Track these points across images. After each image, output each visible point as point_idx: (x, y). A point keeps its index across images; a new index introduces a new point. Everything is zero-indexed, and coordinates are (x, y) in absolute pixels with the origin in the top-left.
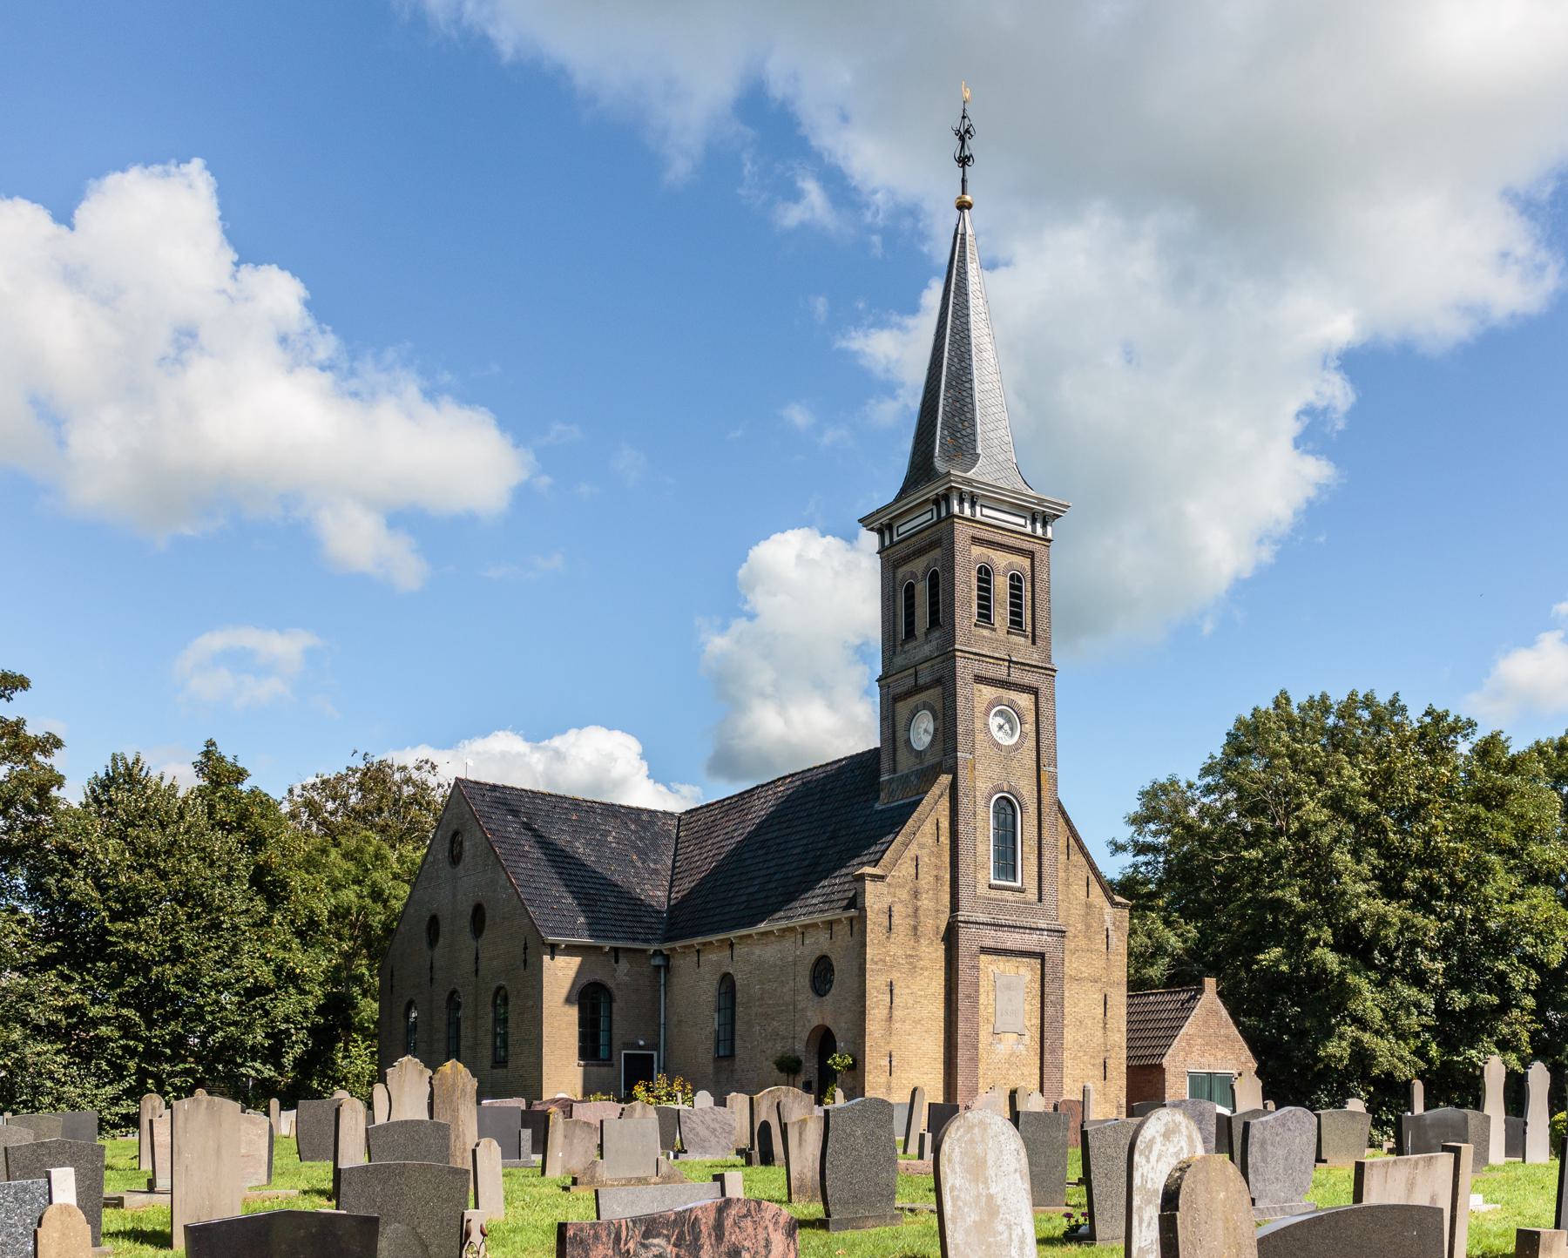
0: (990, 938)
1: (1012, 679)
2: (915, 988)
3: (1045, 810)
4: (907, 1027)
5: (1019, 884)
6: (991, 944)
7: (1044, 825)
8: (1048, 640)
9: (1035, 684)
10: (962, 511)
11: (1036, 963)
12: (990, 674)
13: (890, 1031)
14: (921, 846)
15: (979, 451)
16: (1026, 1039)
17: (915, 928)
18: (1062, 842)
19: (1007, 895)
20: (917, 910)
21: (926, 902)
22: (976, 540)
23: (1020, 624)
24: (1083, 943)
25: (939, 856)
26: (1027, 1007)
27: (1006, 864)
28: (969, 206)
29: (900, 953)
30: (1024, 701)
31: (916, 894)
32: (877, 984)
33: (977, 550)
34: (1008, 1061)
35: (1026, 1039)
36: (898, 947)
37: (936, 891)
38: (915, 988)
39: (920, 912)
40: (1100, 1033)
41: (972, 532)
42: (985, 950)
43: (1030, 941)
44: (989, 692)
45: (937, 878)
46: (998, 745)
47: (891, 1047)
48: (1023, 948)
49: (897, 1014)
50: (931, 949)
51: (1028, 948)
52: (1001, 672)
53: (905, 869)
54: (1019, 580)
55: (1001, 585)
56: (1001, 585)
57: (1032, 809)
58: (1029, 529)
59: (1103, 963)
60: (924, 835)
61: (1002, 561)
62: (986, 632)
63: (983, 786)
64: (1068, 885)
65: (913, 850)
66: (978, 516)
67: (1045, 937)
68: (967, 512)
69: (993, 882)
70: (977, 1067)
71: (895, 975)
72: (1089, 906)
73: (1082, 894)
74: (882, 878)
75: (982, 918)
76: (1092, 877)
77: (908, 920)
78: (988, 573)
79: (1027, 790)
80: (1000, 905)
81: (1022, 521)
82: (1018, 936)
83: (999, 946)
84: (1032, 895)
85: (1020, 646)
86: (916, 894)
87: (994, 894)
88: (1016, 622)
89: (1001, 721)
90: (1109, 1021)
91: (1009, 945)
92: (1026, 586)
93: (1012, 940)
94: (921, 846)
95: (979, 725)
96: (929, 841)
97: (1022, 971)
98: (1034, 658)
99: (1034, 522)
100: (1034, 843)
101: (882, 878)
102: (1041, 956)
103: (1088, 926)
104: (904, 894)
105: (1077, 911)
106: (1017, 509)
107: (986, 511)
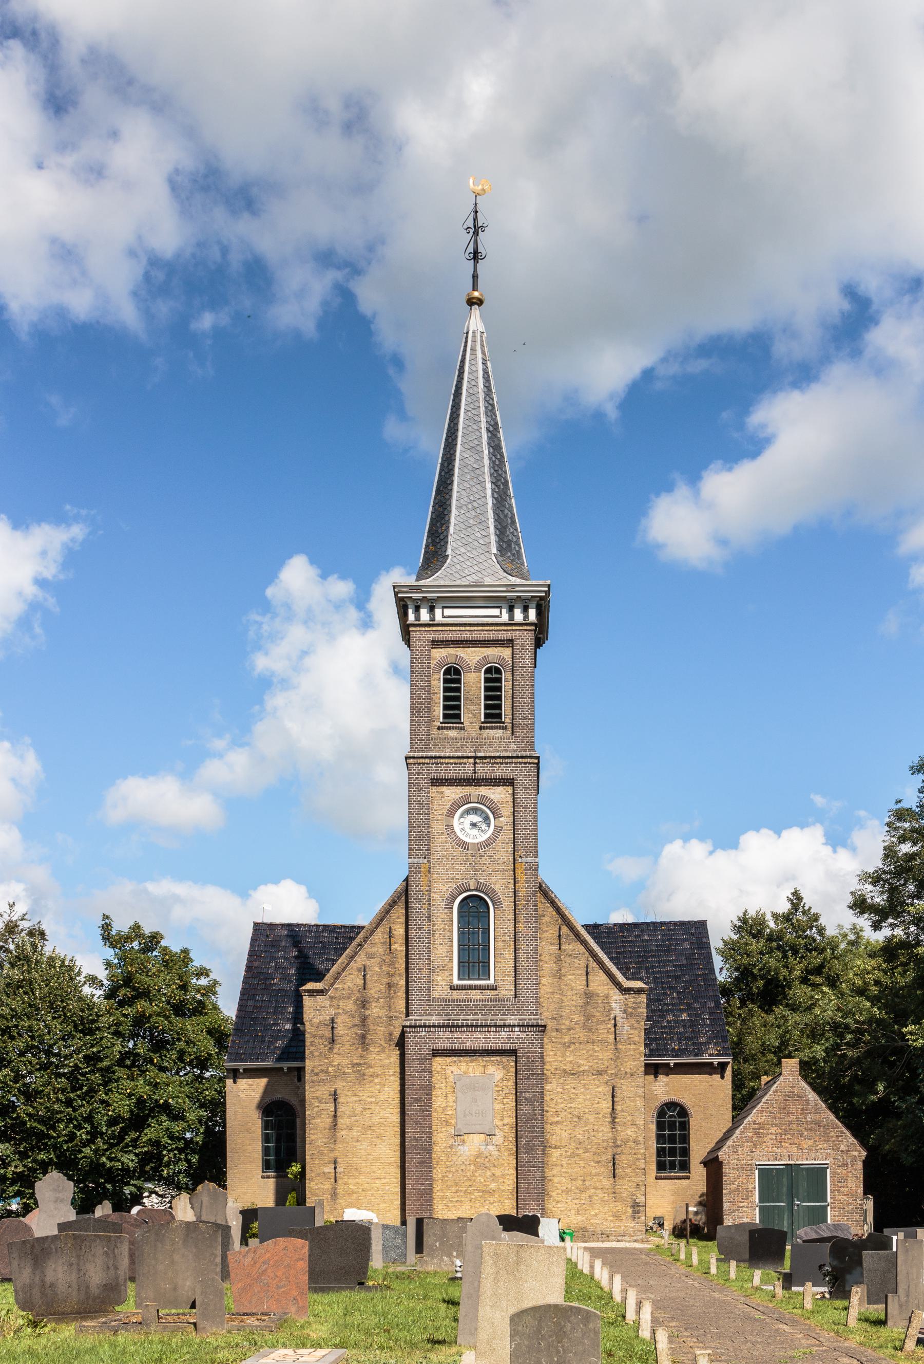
0: (444, 1039)
1: (479, 775)
2: (364, 1095)
3: (522, 903)
4: (355, 1133)
5: (492, 982)
6: (440, 1045)
7: (521, 918)
8: (531, 728)
9: (510, 776)
10: (418, 618)
11: (510, 1062)
12: (451, 775)
13: (334, 1139)
14: (370, 956)
15: (449, 552)
16: (498, 1139)
17: (363, 1037)
18: (550, 933)
19: (475, 995)
20: (364, 1019)
21: (376, 1010)
22: (436, 644)
23: (499, 716)
24: (581, 1035)
25: (392, 964)
26: (498, 1106)
27: (474, 959)
28: (480, 302)
29: (346, 1062)
30: (499, 794)
31: (364, 1004)
32: (319, 1094)
33: (439, 654)
34: (474, 1162)
35: (498, 1139)
36: (342, 1058)
37: (389, 998)
38: (364, 1095)
39: (369, 1021)
40: (607, 1128)
41: (431, 636)
42: (436, 1053)
43: (499, 1039)
44: (452, 793)
45: (389, 986)
46: (464, 845)
47: (337, 1154)
49: (342, 1122)
50: (383, 1056)
51: (500, 1046)
52: (467, 770)
53: (351, 980)
54: (498, 671)
55: (473, 684)
56: (473, 684)
57: (507, 903)
58: (505, 617)
59: (609, 1054)
60: (374, 945)
61: (472, 656)
62: (452, 734)
64: (558, 975)
65: (361, 960)
66: (439, 617)
68: (425, 616)
69: (456, 982)
70: (430, 1169)
71: (339, 1084)
72: (589, 996)
73: (580, 984)
74: (321, 992)
75: (434, 1020)
77: (355, 1030)
78: (457, 672)
79: (500, 884)
80: (462, 1006)
81: (496, 612)
83: (457, 1046)
84: (507, 991)
85: (497, 740)
87: (462, 995)
88: (493, 714)
89: (476, 818)
91: (468, 1045)
92: (506, 676)
93: (472, 1040)
94: (370, 956)
95: (437, 827)
96: (380, 950)
97: (491, 1069)
98: (513, 749)
99: (511, 609)
100: (509, 939)
101: (321, 992)
102: (513, 1052)
103: (588, 1017)
104: (350, 1005)
105: (572, 1001)
106: (493, 601)
107: (448, 612)
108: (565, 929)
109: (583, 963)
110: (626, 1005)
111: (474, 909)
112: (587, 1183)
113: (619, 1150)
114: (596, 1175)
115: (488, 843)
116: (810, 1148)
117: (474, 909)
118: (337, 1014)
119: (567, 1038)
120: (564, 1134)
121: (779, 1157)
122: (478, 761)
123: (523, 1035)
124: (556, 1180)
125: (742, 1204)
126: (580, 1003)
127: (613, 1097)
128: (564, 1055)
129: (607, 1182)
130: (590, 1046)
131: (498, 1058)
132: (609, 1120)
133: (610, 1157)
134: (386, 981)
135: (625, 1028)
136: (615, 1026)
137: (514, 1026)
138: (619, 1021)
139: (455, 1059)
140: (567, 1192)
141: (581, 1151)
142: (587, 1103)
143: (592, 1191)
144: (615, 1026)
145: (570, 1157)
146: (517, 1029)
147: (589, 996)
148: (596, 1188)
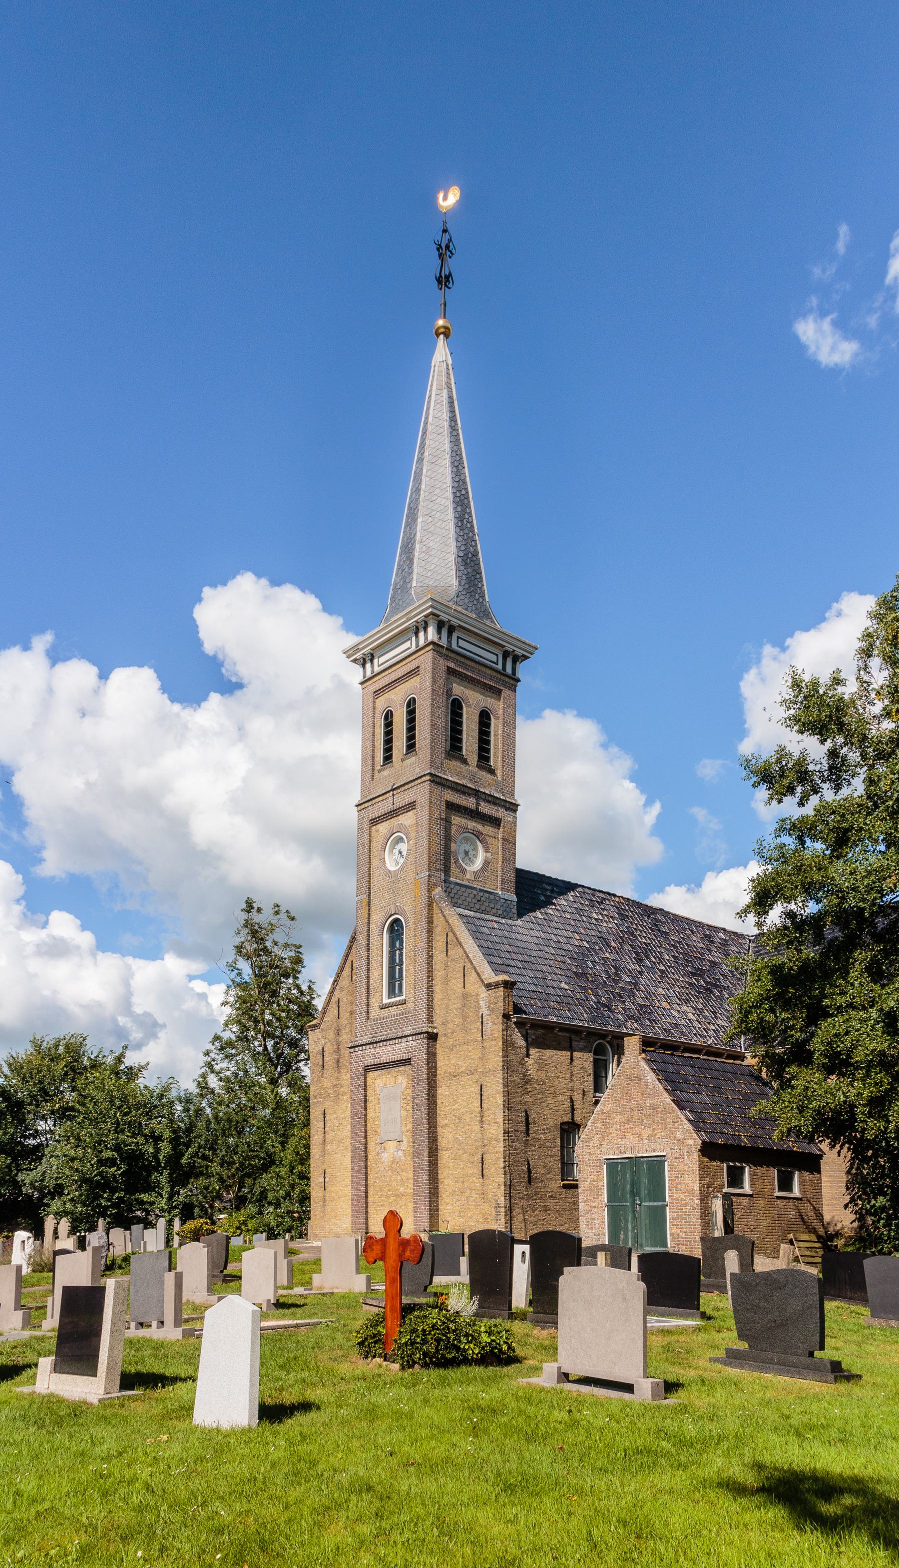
1: (396, 806)
6: (370, 1061)
17: (338, 1061)
26: (404, 1114)
31: (338, 1033)
35: (404, 1145)
40: (477, 1128)
42: (368, 1069)
44: (383, 828)
48: (396, 1058)
63: (377, 917)
67: (411, 1042)
69: (386, 1001)
76: (468, 965)
82: (389, 1048)
83: (377, 1061)
86: (338, 1033)
90: (486, 1113)
91: (385, 1059)
93: (387, 1053)
103: (465, 1017)
104: (331, 1035)
108: (450, 934)
109: (461, 966)
110: (490, 1001)
111: (396, 929)
112: (466, 1185)
113: (486, 1149)
114: (472, 1175)
115: (402, 868)
116: (649, 1137)
117: (396, 929)
118: (325, 1043)
119: (451, 1042)
120: (451, 1137)
121: (623, 1150)
122: (395, 792)
123: (414, 1044)
124: (446, 1182)
125: (594, 1204)
126: (459, 1005)
127: (481, 1095)
128: (449, 1059)
129: (477, 1182)
130: (466, 1047)
131: (403, 1068)
132: (478, 1119)
133: (480, 1157)
134: (349, 1009)
135: (489, 1026)
136: (482, 1023)
137: (408, 1036)
138: (485, 1018)
139: (379, 1072)
140: (453, 1193)
141: (461, 1152)
142: (465, 1104)
143: (469, 1192)
144: (482, 1023)
145: (455, 1158)
146: (410, 1038)
147: (465, 996)
148: (471, 1189)
